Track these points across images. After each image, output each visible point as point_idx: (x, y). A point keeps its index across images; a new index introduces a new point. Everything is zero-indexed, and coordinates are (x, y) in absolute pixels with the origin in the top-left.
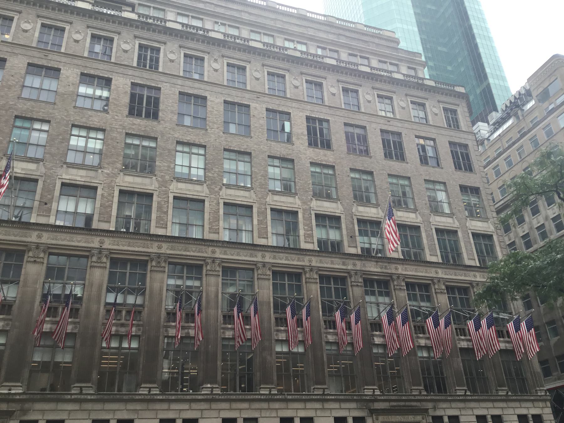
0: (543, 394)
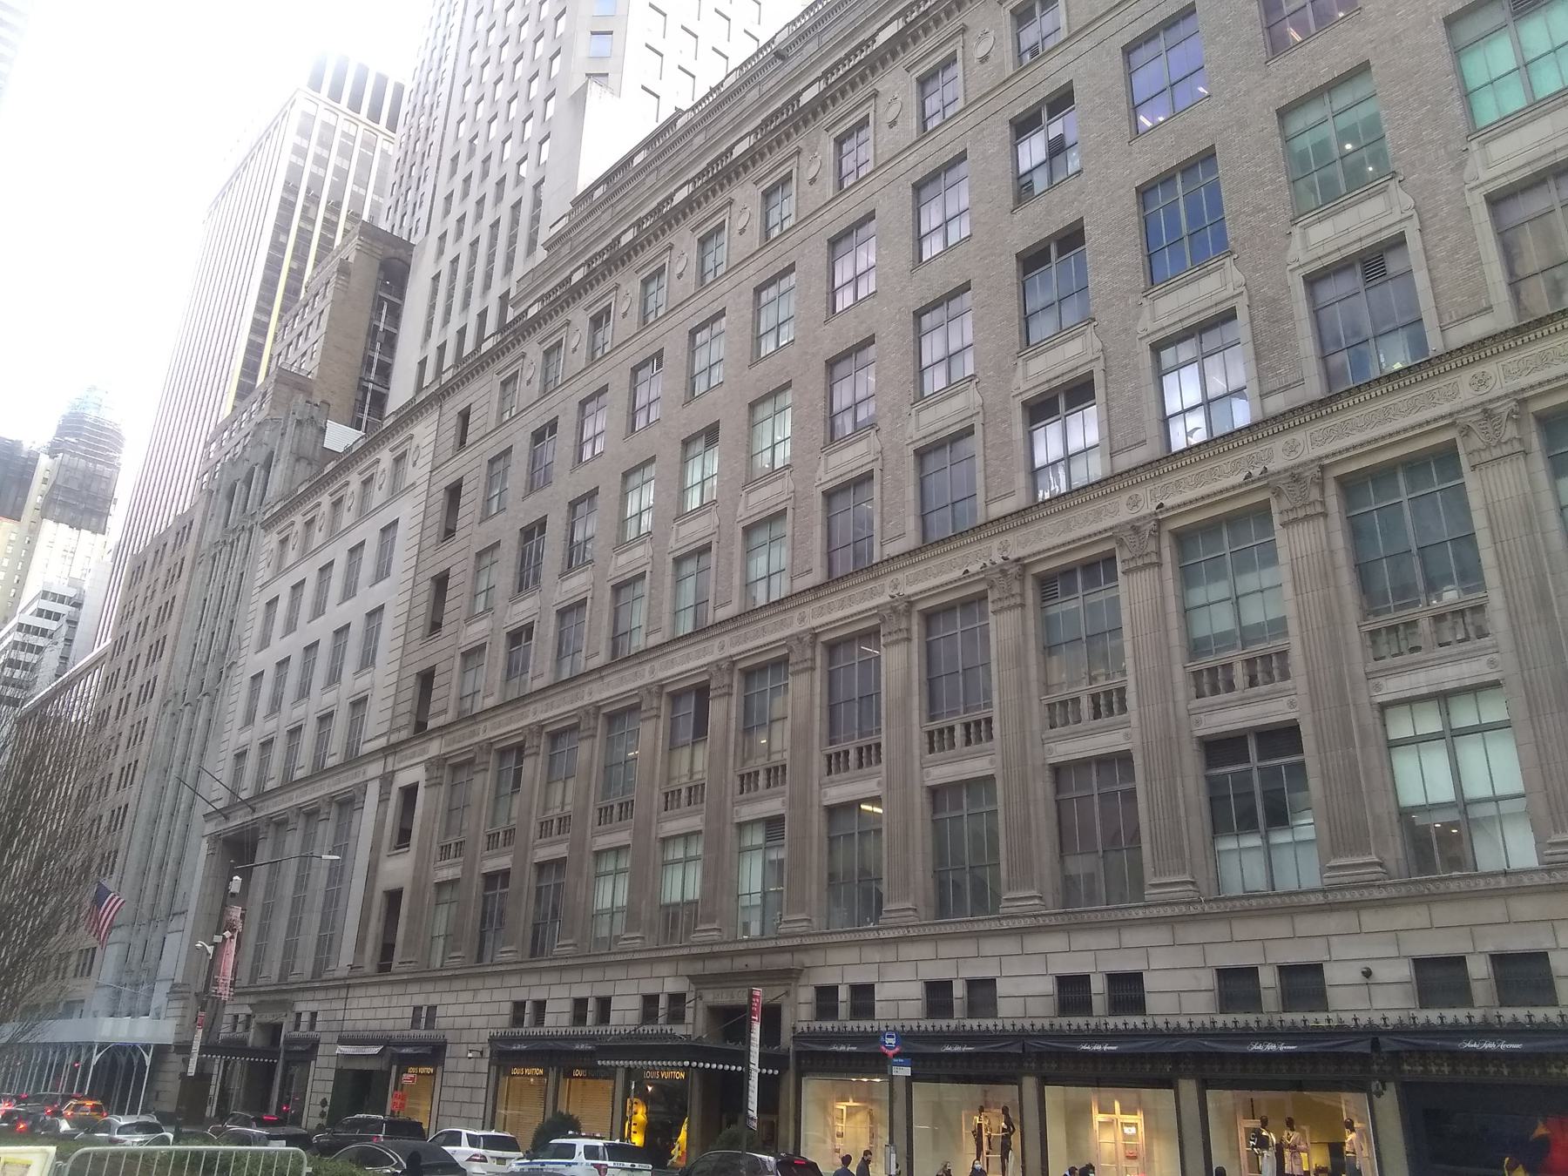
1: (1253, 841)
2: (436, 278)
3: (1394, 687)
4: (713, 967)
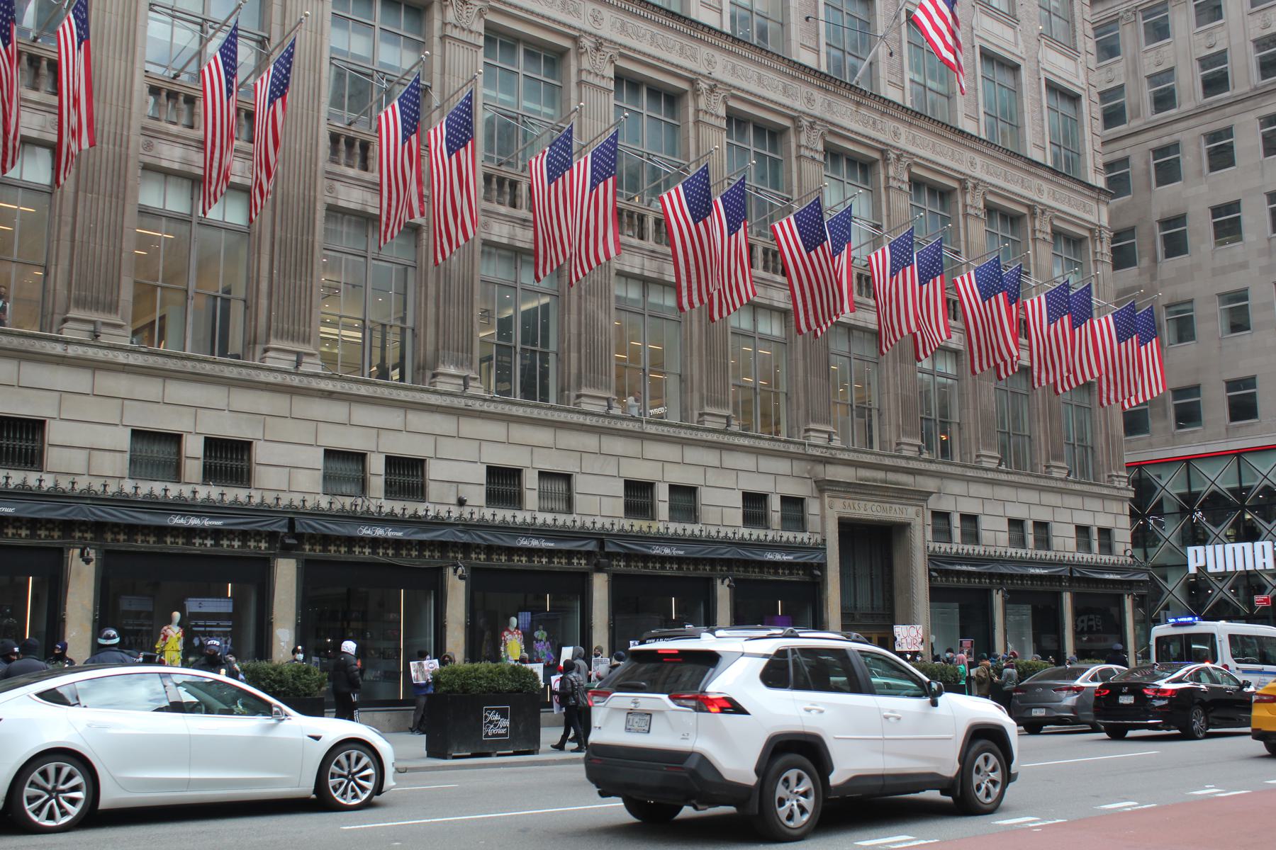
0: (1123, 485)
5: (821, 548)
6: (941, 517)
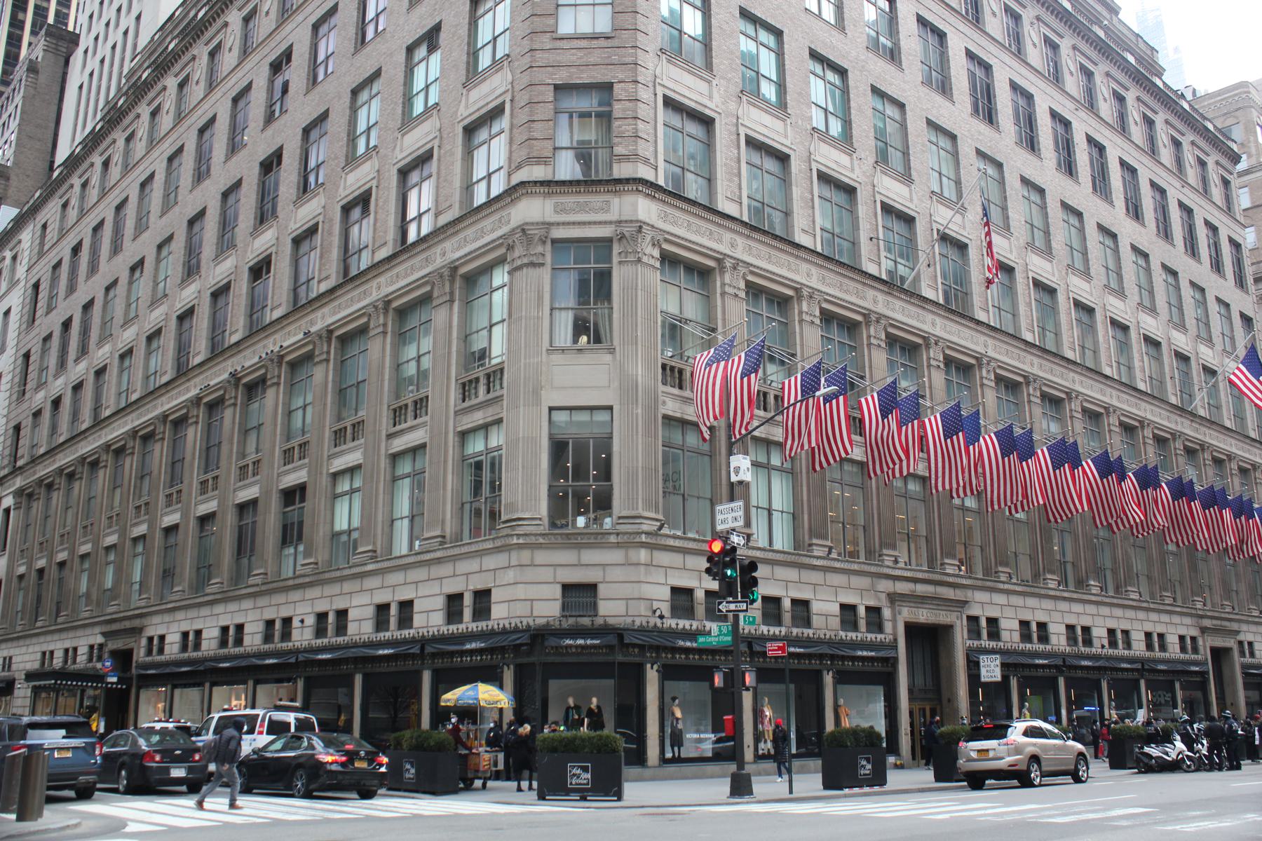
1: (292, 550)
2: (81, 87)
3: (339, 464)
4: (115, 627)
5: (894, 646)
6: (973, 620)
